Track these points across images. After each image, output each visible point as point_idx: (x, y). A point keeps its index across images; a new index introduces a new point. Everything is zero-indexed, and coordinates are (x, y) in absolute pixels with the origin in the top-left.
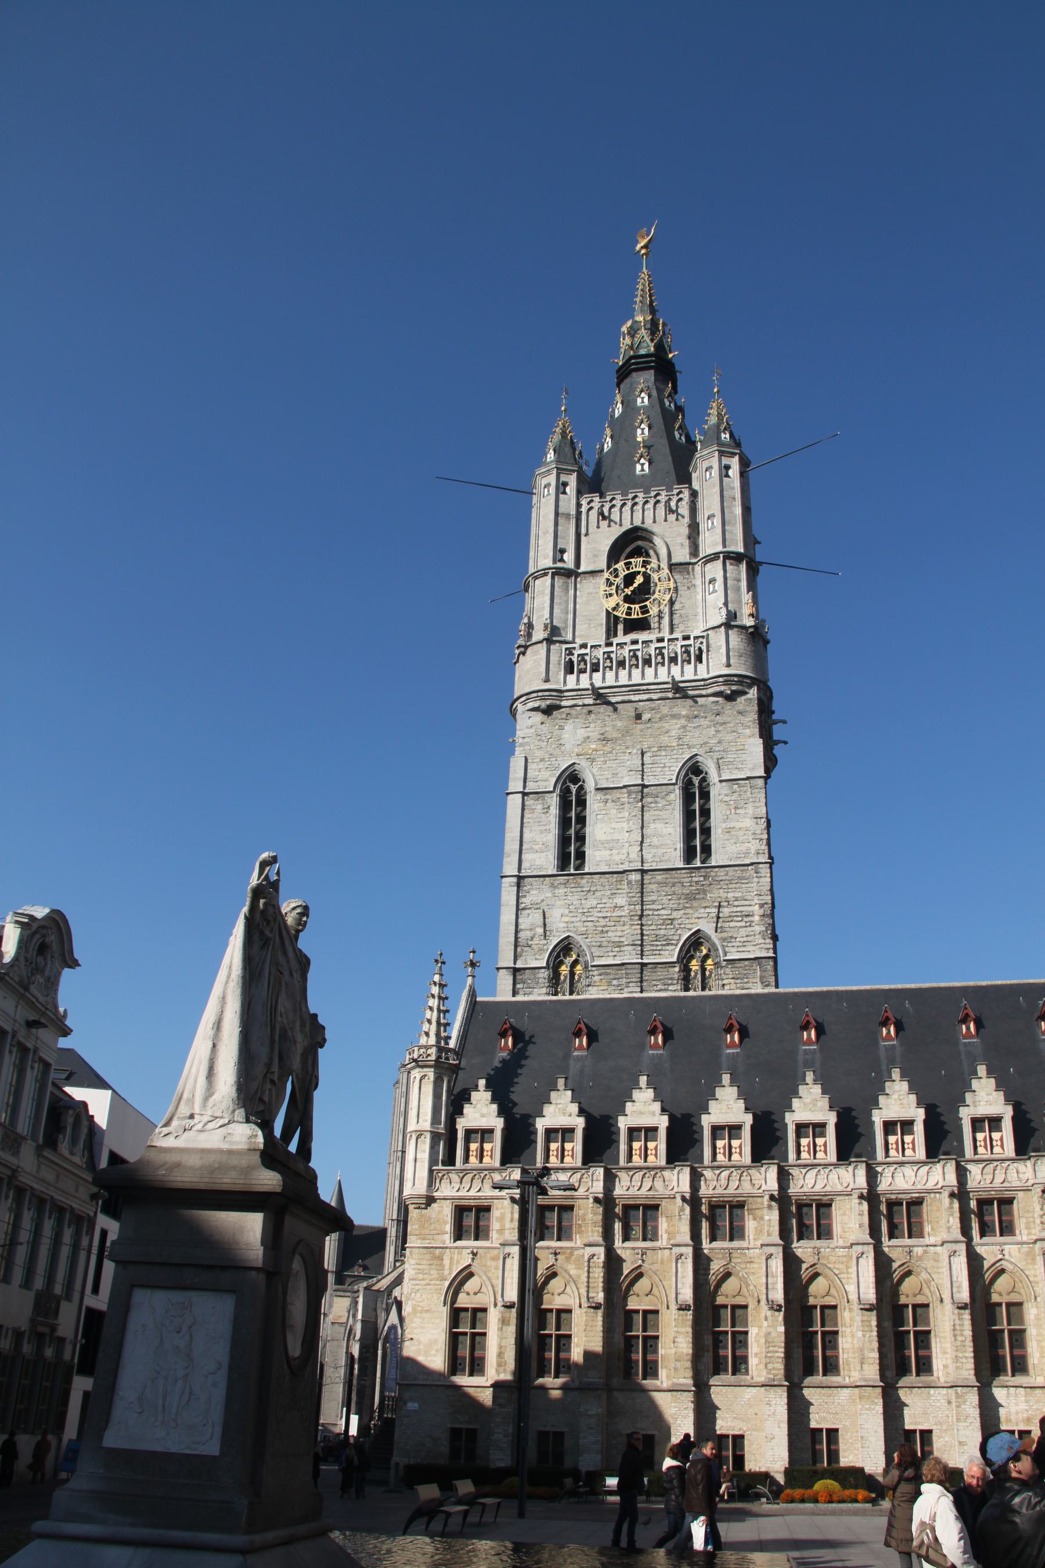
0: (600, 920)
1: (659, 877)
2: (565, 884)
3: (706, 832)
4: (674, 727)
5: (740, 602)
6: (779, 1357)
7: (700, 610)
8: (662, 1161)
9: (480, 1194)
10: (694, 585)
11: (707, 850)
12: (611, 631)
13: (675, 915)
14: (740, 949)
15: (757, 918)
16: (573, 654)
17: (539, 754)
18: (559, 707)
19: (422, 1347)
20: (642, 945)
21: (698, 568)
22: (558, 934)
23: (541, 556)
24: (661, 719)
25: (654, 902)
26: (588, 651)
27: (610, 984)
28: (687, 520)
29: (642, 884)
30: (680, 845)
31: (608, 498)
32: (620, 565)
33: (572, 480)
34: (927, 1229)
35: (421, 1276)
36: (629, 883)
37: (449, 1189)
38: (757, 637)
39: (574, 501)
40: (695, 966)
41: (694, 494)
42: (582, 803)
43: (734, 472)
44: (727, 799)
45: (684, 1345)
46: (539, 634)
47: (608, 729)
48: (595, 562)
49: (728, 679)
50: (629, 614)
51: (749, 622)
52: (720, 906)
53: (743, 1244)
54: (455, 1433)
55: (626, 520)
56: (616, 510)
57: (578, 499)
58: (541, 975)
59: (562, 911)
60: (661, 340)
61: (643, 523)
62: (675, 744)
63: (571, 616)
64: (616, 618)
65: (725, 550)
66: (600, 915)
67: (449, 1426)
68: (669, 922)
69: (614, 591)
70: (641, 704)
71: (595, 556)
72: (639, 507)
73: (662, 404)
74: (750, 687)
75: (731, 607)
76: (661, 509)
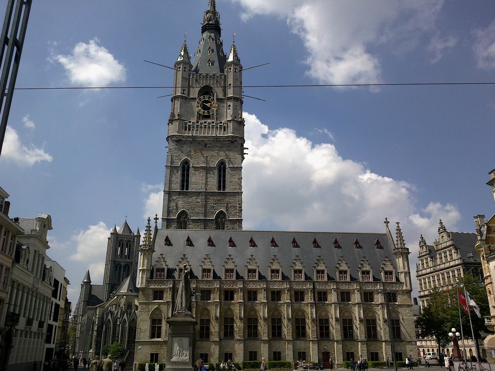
0: (193, 205)
1: (210, 194)
2: (182, 194)
3: (224, 181)
6: (242, 332)
9: (161, 287)
10: (224, 106)
11: (224, 187)
13: (215, 205)
14: (233, 216)
15: (238, 208)
16: (187, 124)
17: (176, 155)
19: (143, 330)
22: (180, 209)
24: (212, 147)
25: (208, 201)
26: (191, 124)
31: (198, 75)
32: (202, 97)
34: (282, 299)
35: (143, 310)
39: (188, 74)
41: (225, 76)
42: (188, 170)
44: (231, 172)
45: (217, 329)
48: (194, 95)
50: (204, 113)
52: (227, 204)
53: (233, 302)
54: (152, 355)
58: (175, 221)
59: (181, 202)
62: (216, 155)
64: (200, 114)
66: (192, 204)
67: (150, 353)
68: (213, 207)
69: (199, 106)
70: (207, 142)
71: (194, 93)
73: (216, 41)
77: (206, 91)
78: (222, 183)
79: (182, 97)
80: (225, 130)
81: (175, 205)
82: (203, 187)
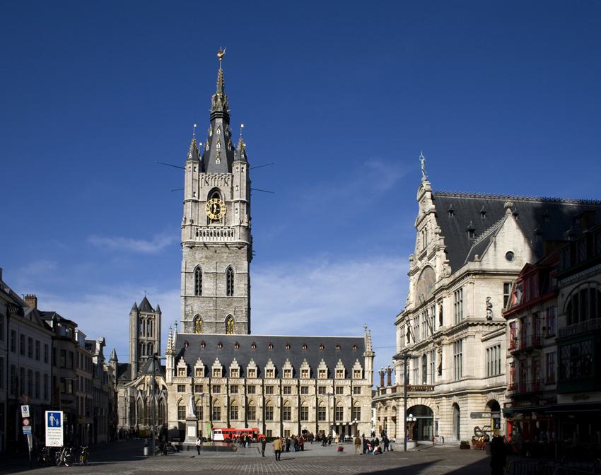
3: (232, 287)
4: (225, 255)
5: (244, 217)
8: (221, 376)
11: (232, 292)
12: (208, 223)
17: (189, 261)
18: (194, 247)
23: (188, 196)
30: (226, 291)
32: (211, 200)
37: (177, 381)
38: (248, 229)
40: (229, 323)
41: (233, 176)
42: (201, 276)
43: (245, 170)
49: (239, 243)
51: (246, 225)
55: (213, 184)
76: (223, 182)
77: (215, 193)
78: (230, 289)
79: (193, 201)
82: (214, 293)
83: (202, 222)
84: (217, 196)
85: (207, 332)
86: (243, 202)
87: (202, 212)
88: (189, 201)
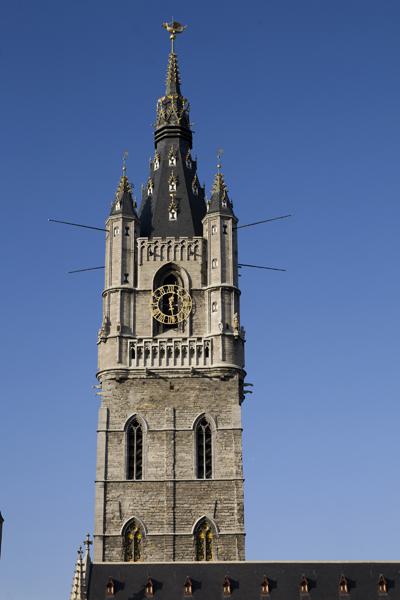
3: (209, 457)
4: (193, 394)
5: (230, 318)
7: (207, 321)
11: (209, 468)
13: (193, 507)
15: (236, 511)
20: (174, 524)
21: (206, 293)
25: (180, 499)
27: (156, 546)
28: (200, 259)
29: (175, 489)
30: (194, 467)
32: (161, 288)
33: (132, 225)
36: (167, 488)
40: (203, 536)
41: (205, 242)
42: (140, 436)
46: (114, 332)
47: (155, 394)
49: (223, 369)
50: (166, 321)
56: (159, 249)
57: (135, 238)
60: (184, 113)
61: (175, 259)
63: (132, 320)
65: (224, 284)
71: (146, 280)
72: (172, 249)
73: (184, 163)
74: (235, 374)
75: (227, 321)
78: (204, 465)
79: (124, 291)
80: (207, 355)
81: (117, 509)
82: (170, 472)
83: (144, 330)
84: (173, 279)
85: (152, 557)
86: (225, 291)
87: (141, 311)
88: (116, 290)
